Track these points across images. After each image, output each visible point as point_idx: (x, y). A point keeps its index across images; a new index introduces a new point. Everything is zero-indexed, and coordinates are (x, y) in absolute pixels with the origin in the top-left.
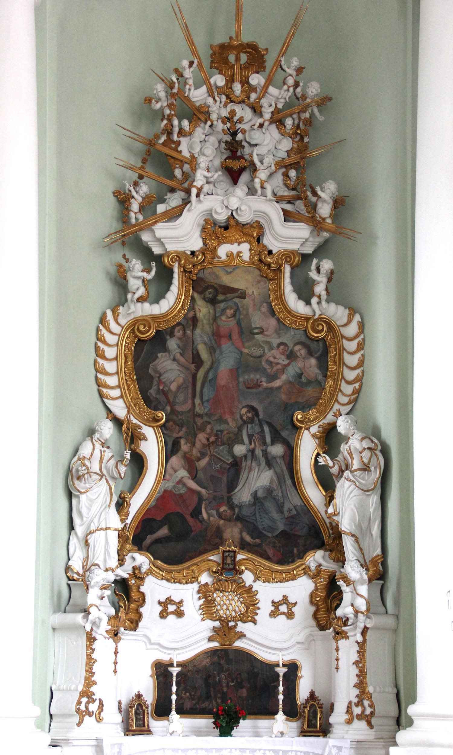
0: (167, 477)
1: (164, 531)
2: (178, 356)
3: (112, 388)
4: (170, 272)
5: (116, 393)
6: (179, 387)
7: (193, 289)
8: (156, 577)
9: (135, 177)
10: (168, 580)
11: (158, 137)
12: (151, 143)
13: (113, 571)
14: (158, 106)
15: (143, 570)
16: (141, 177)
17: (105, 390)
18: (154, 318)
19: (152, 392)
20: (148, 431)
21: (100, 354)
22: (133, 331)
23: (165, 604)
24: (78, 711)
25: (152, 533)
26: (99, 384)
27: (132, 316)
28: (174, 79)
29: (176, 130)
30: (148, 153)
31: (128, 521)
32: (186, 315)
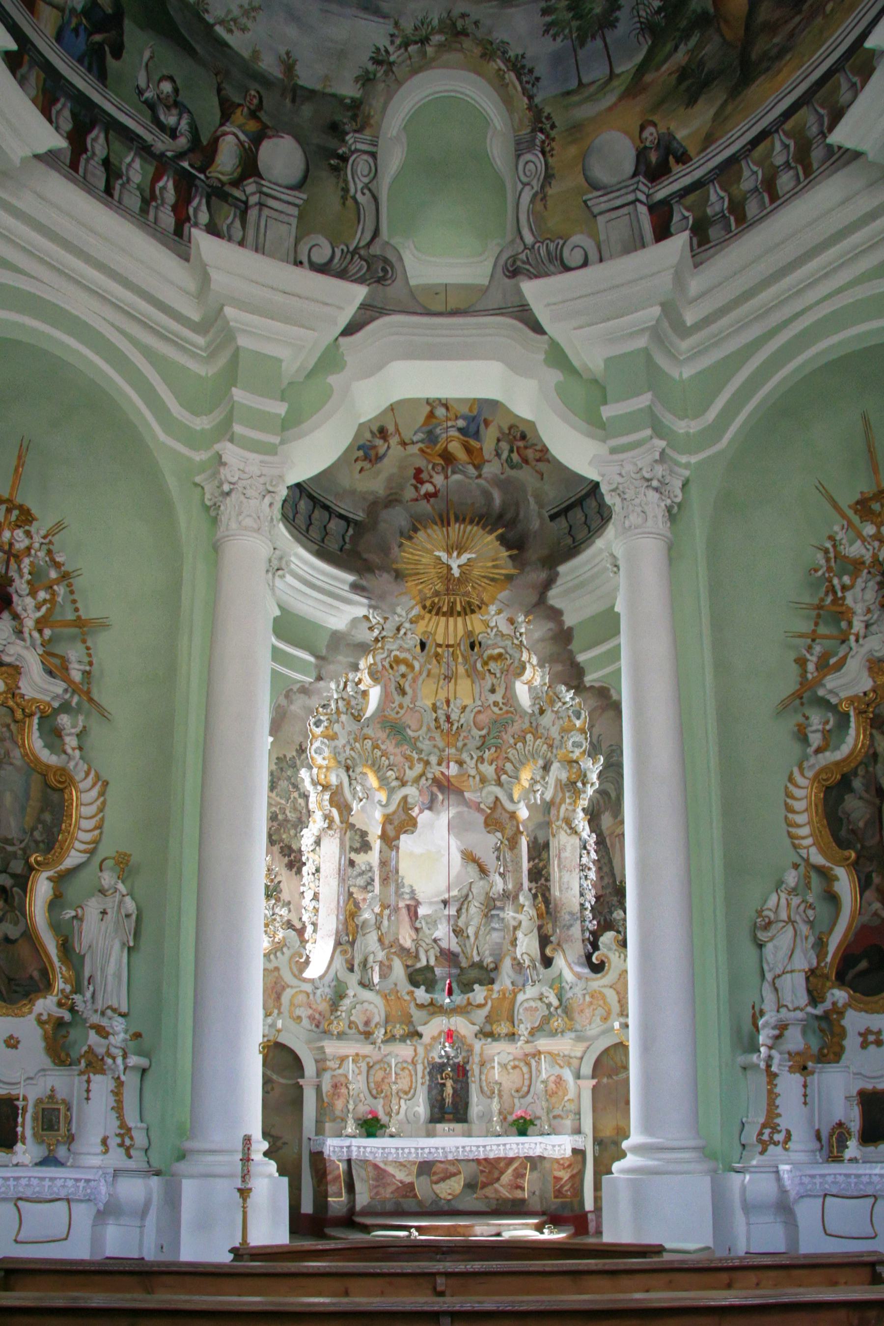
0: (863, 911)
1: (863, 965)
2: (865, 795)
3: (803, 838)
4: (847, 715)
5: (809, 841)
6: (866, 824)
7: (871, 727)
8: (855, 1010)
9: (809, 641)
10: (866, 1012)
11: (822, 600)
12: (820, 607)
13: (802, 1010)
14: (820, 573)
15: (840, 1004)
16: (813, 640)
17: (796, 842)
18: (837, 764)
19: (843, 833)
20: (841, 872)
21: (790, 809)
22: (819, 782)
23: (864, 1035)
24: (760, 1141)
25: (854, 966)
26: (791, 836)
27: (817, 768)
28: (828, 545)
29: (838, 588)
30: (819, 616)
31: (829, 959)
32: (866, 753)
